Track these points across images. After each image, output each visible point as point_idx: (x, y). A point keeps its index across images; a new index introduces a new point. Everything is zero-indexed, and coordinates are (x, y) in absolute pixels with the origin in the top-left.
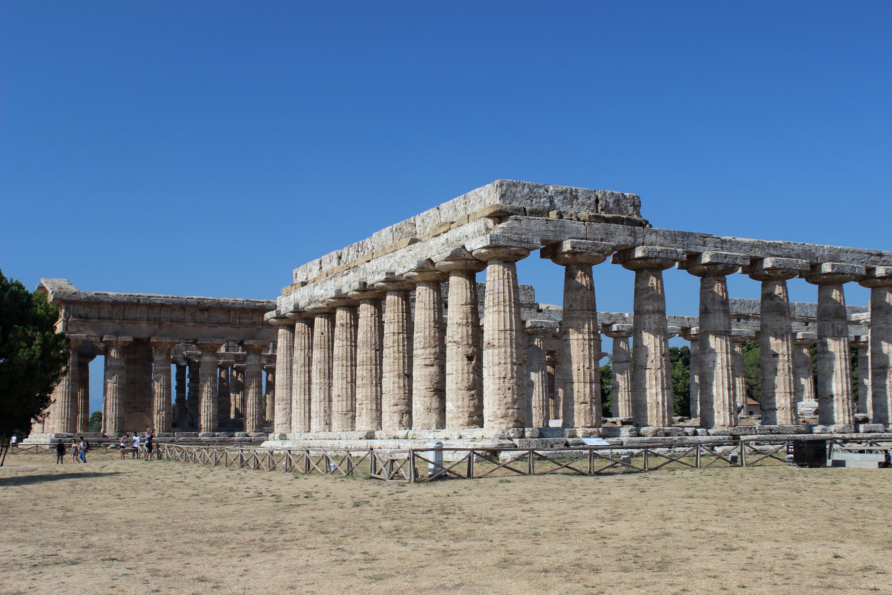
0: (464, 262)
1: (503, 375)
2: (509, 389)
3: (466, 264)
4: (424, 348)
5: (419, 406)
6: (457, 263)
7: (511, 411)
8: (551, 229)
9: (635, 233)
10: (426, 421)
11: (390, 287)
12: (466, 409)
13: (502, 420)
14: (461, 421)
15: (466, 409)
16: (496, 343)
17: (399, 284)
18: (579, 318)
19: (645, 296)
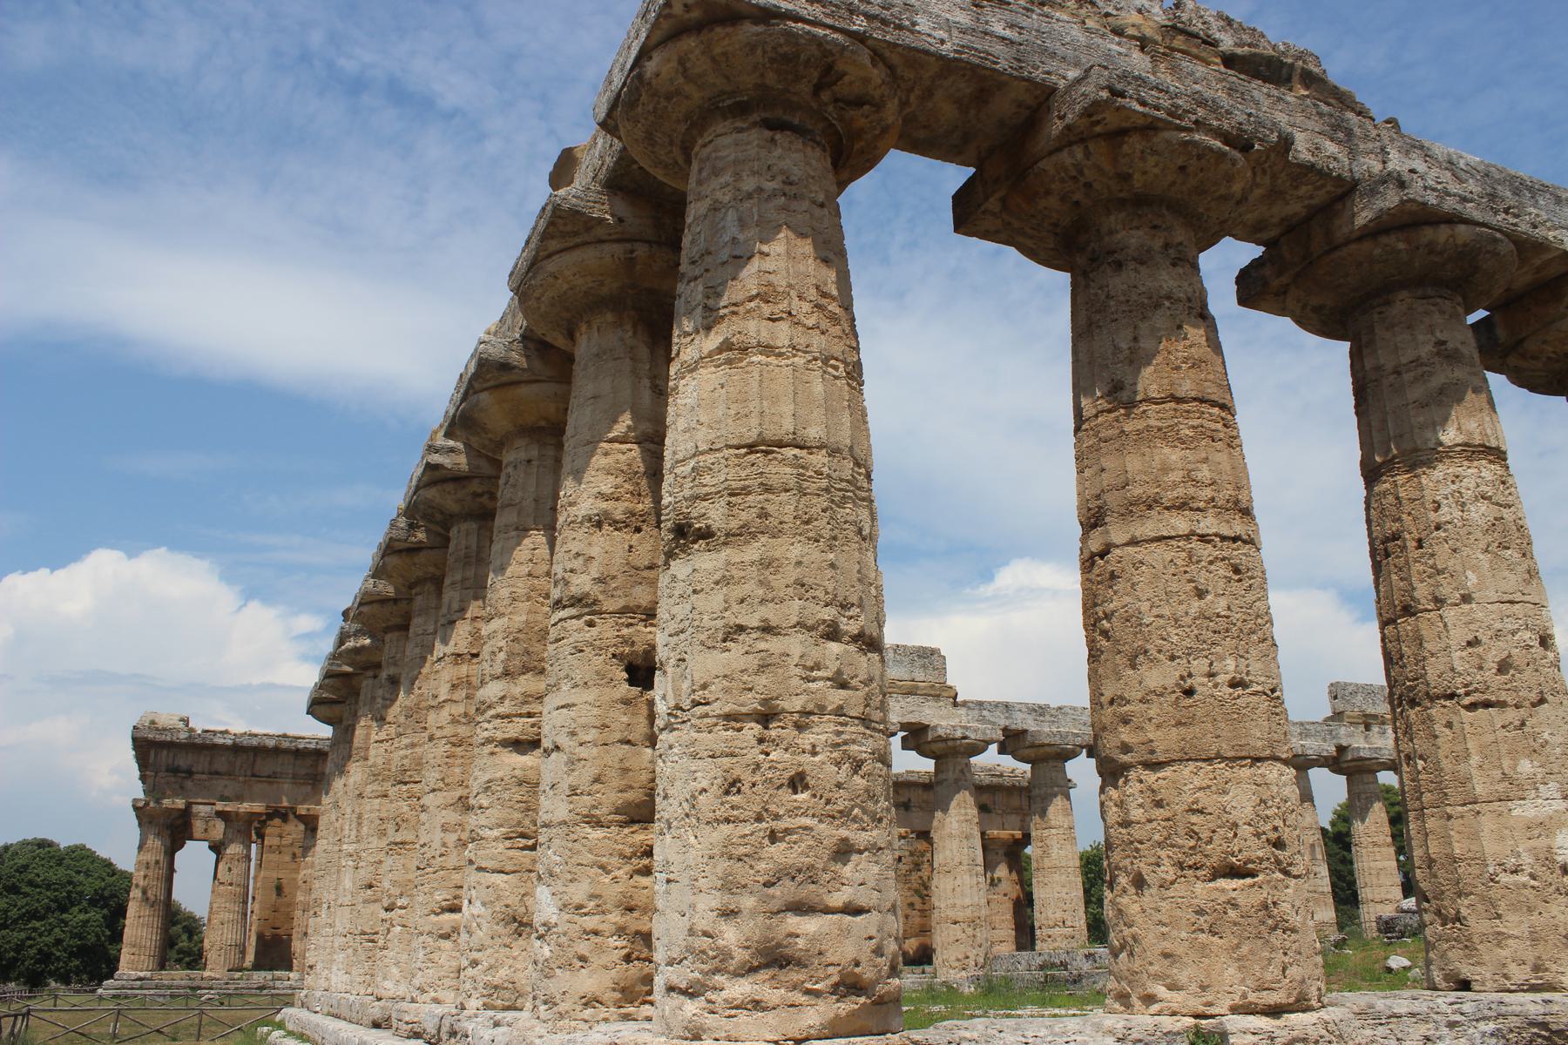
0: (618, 249)
1: (751, 703)
2: (797, 782)
3: (630, 262)
4: (506, 674)
5: (477, 909)
6: (589, 255)
7: (809, 925)
8: (998, 28)
9: (1349, 133)
10: (502, 974)
11: (451, 505)
12: (615, 917)
13: (740, 989)
14: (589, 981)
15: (615, 917)
16: (715, 515)
17: (475, 486)
18: (1167, 435)
19: (1416, 393)
